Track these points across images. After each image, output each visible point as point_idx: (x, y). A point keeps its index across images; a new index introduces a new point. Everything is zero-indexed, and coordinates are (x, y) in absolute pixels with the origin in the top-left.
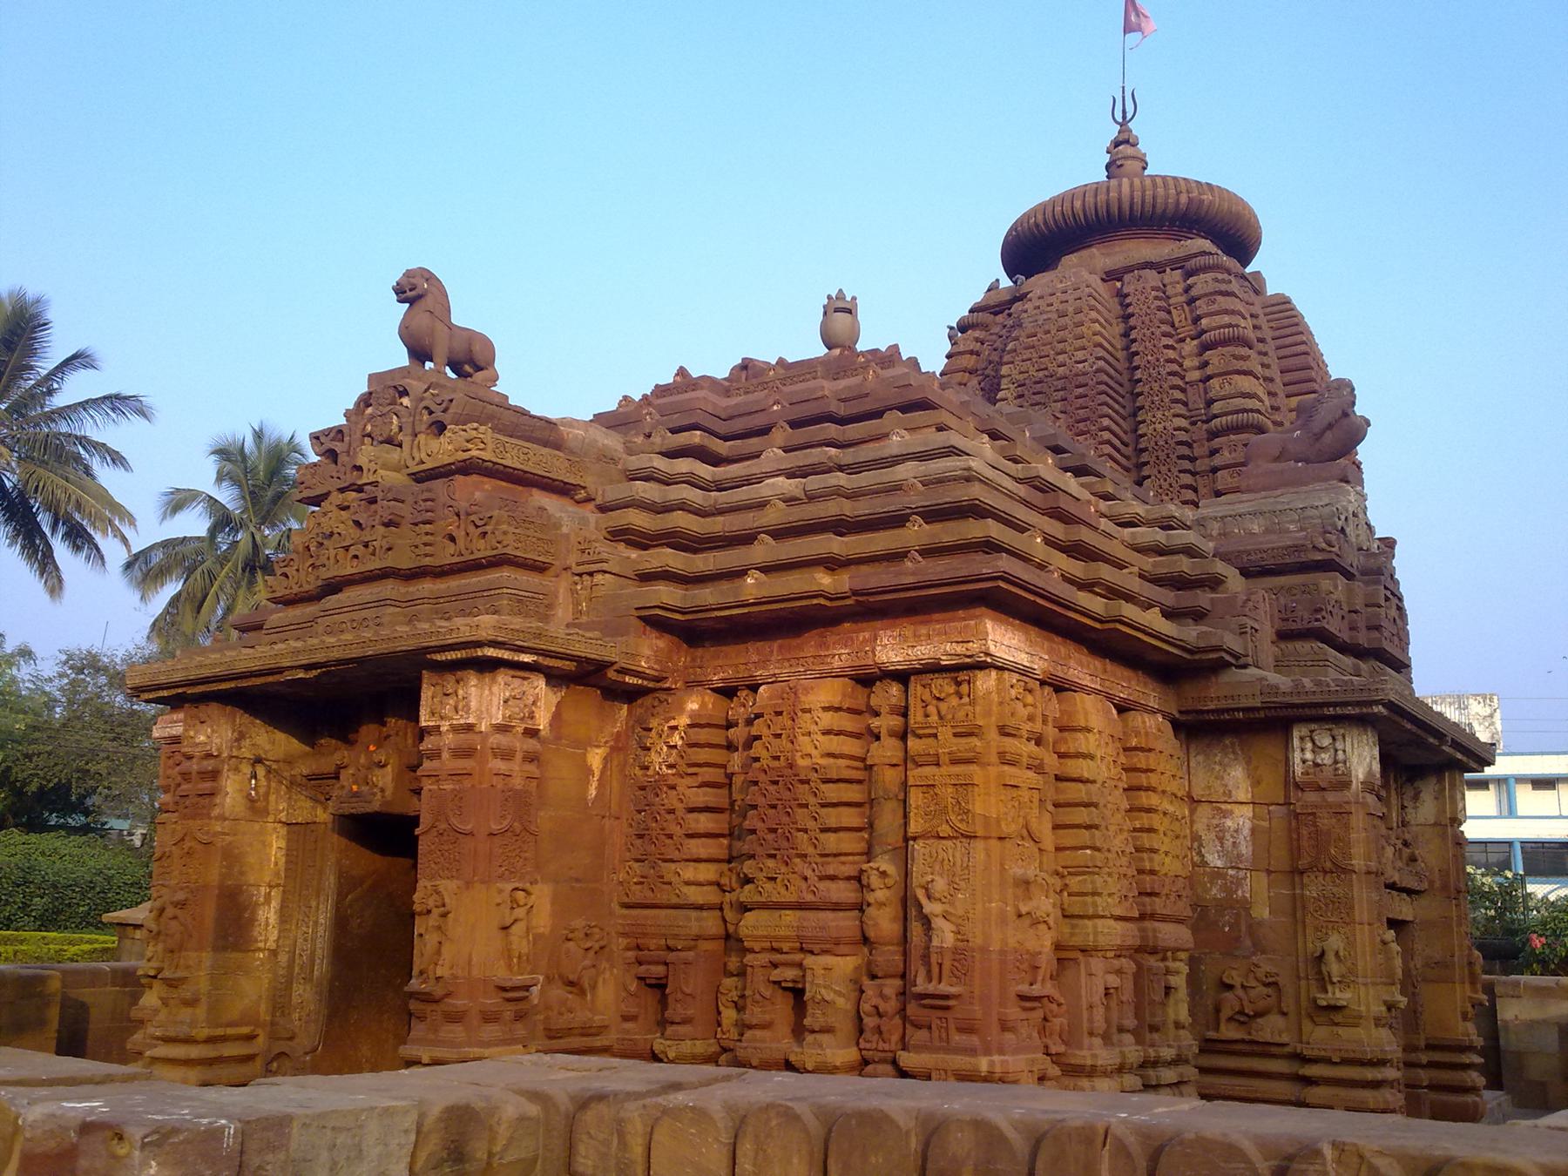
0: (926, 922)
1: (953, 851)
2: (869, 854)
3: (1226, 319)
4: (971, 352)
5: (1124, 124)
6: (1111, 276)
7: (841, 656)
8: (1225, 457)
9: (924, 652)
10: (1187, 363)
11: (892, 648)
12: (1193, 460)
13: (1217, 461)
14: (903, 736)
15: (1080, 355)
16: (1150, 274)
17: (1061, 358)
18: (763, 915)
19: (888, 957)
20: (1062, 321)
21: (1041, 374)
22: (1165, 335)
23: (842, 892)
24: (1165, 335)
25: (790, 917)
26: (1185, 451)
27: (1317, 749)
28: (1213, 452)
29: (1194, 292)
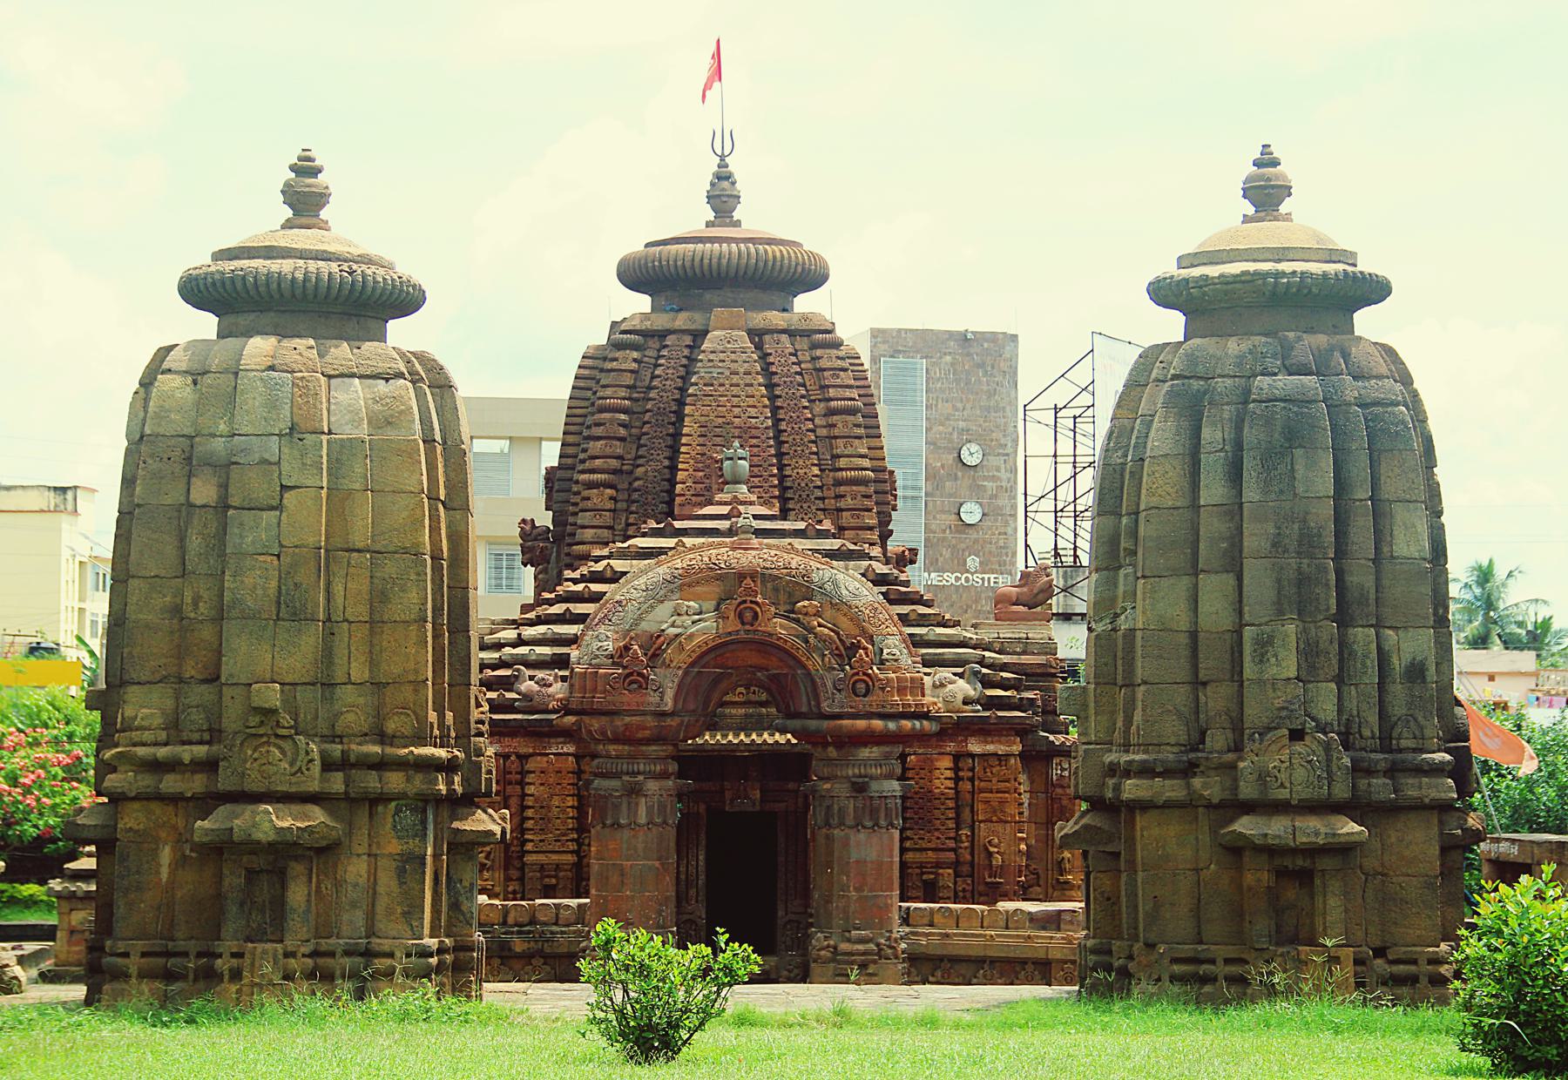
0: (990, 854)
1: (999, 828)
2: (958, 828)
3: (848, 393)
4: (632, 371)
5: (722, 157)
6: (757, 335)
7: (951, 747)
8: (848, 502)
9: (991, 748)
10: (817, 421)
11: (975, 747)
12: (822, 499)
13: (842, 504)
14: (972, 780)
15: (753, 412)
16: (784, 337)
17: (736, 410)
18: (918, 855)
19: (965, 869)
20: (735, 379)
21: (720, 420)
22: (803, 397)
23: (951, 844)
24: (803, 397)
25: (930, 853)
26: (818, 493)
27: (1063, 770)
28: (839, 497)
29: (824, 363)
